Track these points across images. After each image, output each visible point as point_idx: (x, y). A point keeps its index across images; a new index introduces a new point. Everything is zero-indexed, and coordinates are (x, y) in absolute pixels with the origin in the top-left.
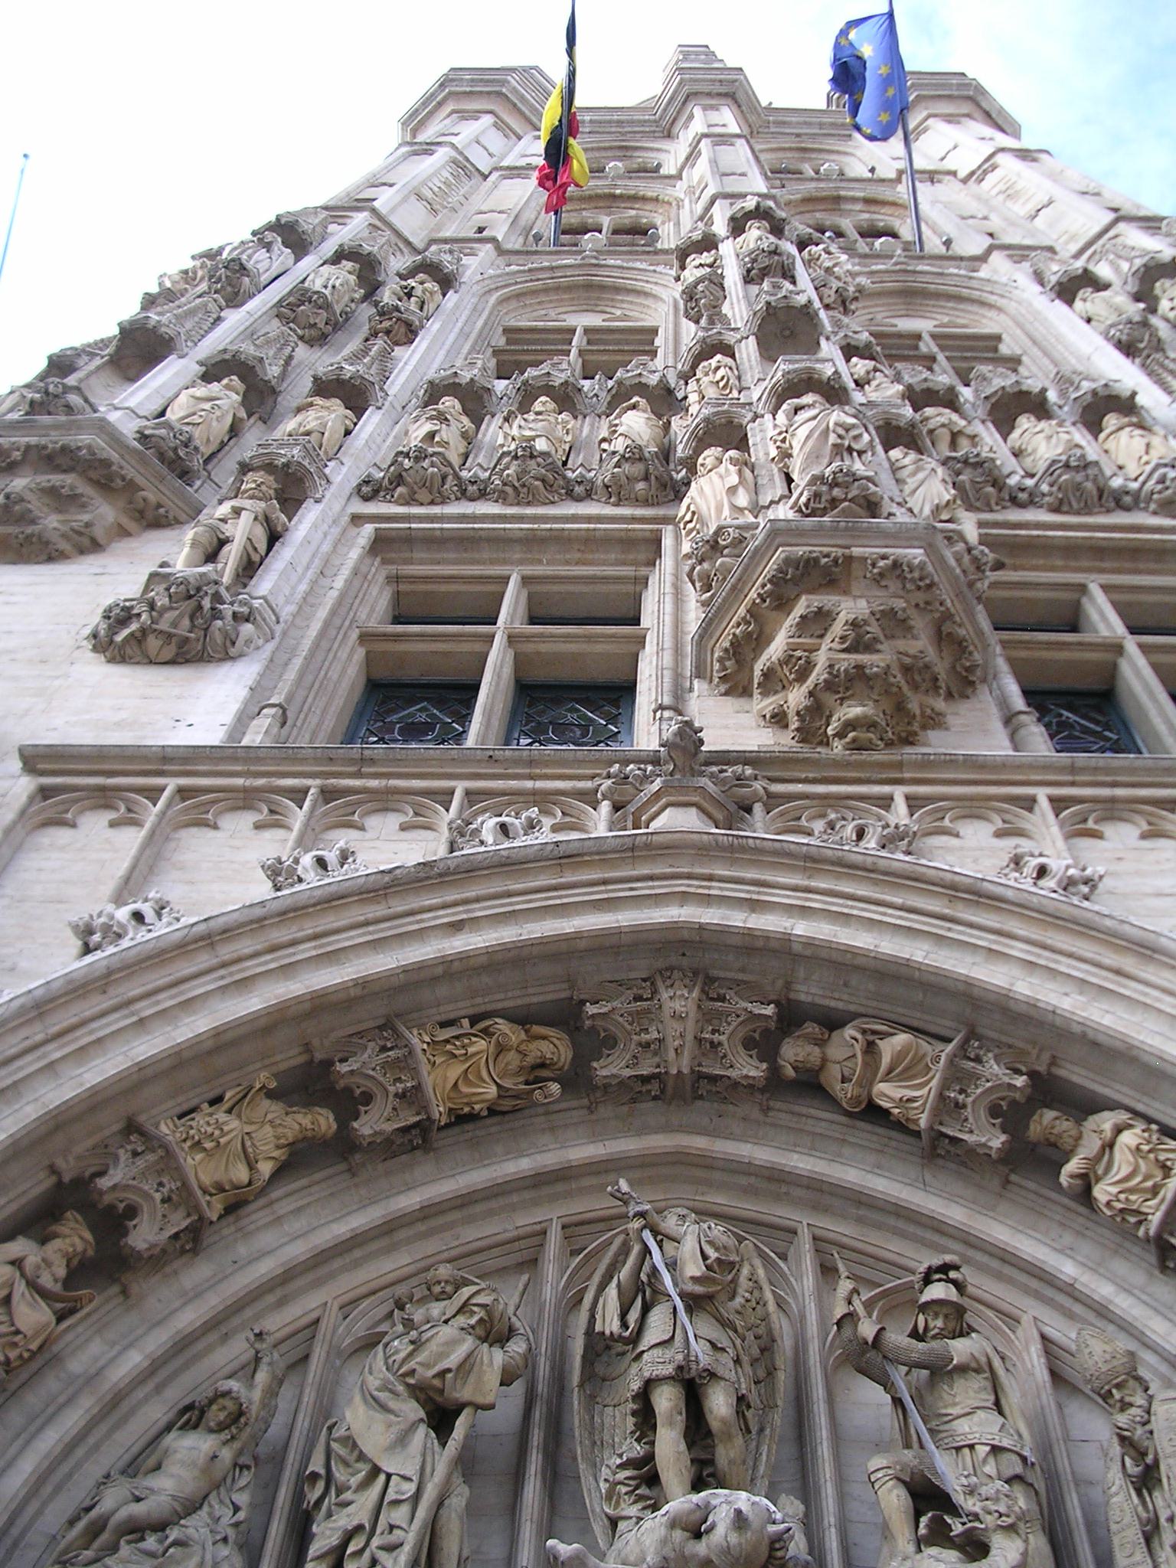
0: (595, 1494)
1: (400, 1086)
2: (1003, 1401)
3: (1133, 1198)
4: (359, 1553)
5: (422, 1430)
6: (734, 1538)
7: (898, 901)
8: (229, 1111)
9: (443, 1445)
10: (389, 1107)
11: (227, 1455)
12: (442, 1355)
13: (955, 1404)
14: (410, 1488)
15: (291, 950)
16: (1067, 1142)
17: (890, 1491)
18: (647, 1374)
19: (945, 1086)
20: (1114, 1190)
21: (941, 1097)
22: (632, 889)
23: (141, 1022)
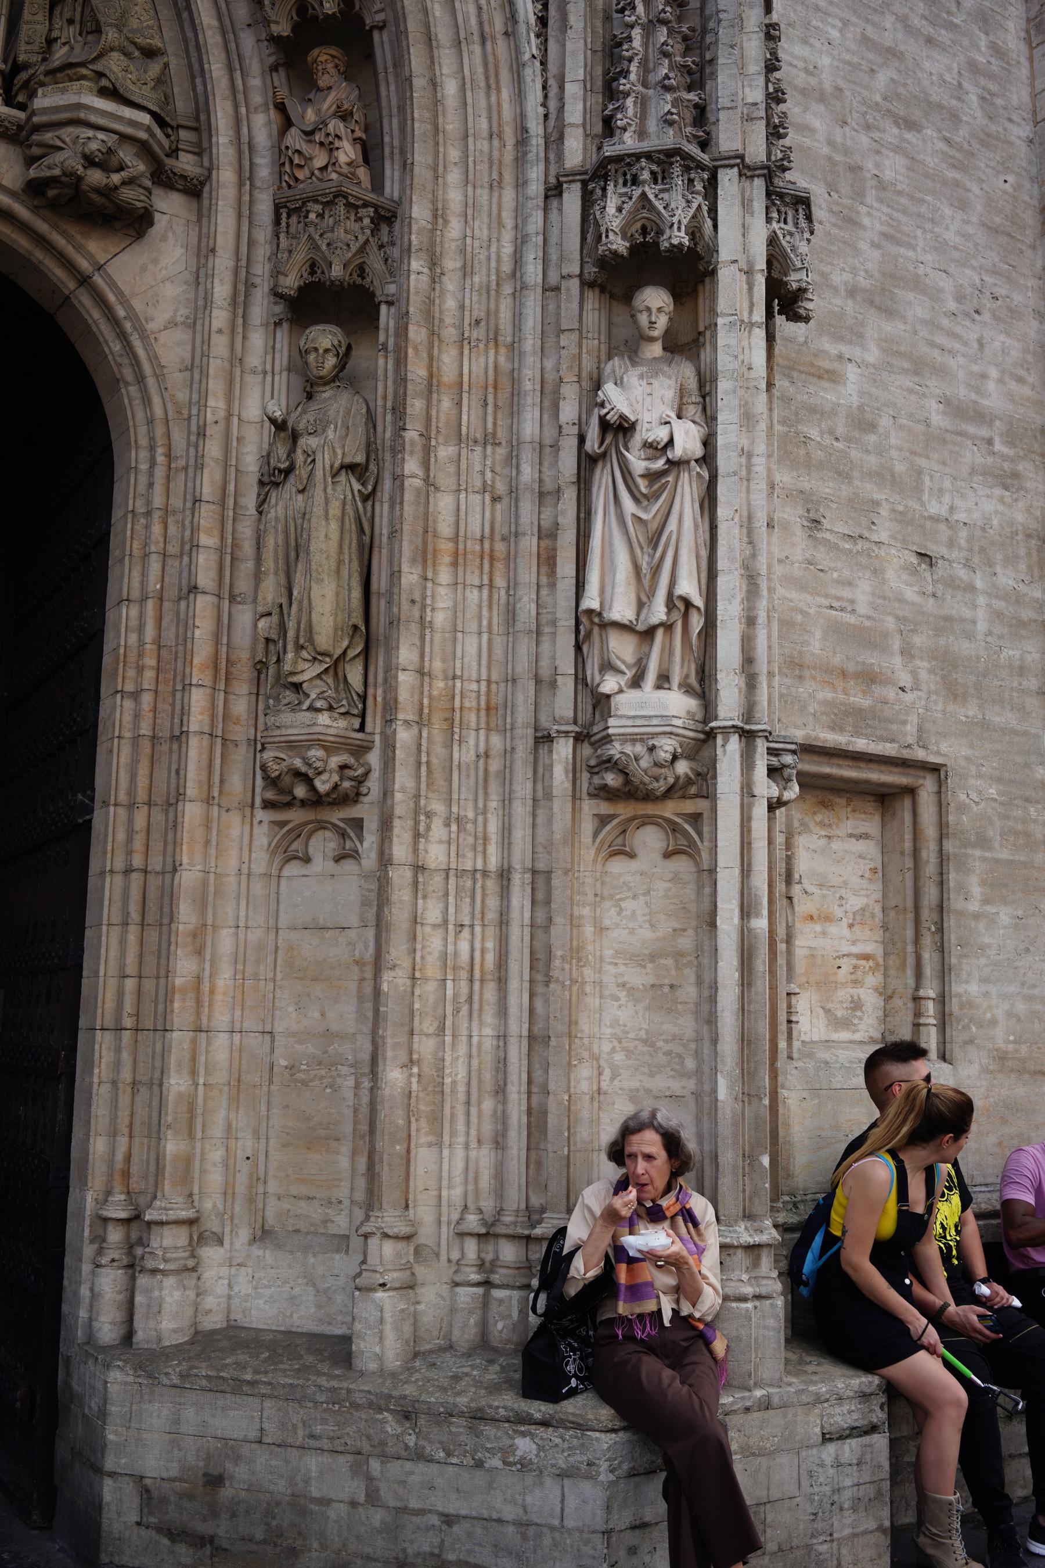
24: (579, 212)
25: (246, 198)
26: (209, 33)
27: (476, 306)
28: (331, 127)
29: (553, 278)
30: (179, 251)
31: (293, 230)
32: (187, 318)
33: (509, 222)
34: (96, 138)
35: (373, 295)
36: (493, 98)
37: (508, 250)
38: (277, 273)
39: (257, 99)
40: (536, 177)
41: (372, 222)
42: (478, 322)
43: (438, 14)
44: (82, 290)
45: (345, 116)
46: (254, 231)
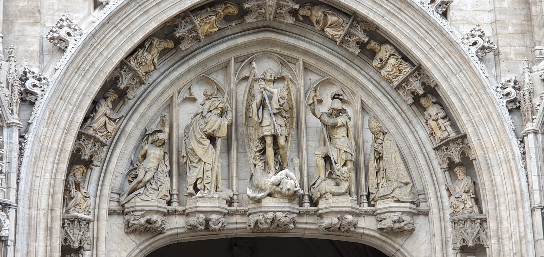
1: (192, 35)
2: (349, 133)
3: (390, 77)
5: (211, 145)
6: (287, 192)
9: (216, 150)
10: (189, 40)
11: (162, 152)
12: (213, 126)
13: (337, 135)
14: (210, 166)
16: (376, 51)
17: (320, 160)
18: (264, 134)
19: (345, 35)
20: (386, 74)
24: (541, 218)
25: (442, 215)
26: (423, 167)
27: (514, 249)
29: (537, 238)
31: (456, 228)
32: (429, 254)
33: (522, 220)
35: (484, 245)
36: (512, 181)
37: (522, 229)
38: (454, 244)
39: (441, 180)
40: (527, 205)
41: (480, 224)
42: (515, 254)
43: (491, 156)
44: (398, 252)
45: (467, 192)
46: (446, 224)
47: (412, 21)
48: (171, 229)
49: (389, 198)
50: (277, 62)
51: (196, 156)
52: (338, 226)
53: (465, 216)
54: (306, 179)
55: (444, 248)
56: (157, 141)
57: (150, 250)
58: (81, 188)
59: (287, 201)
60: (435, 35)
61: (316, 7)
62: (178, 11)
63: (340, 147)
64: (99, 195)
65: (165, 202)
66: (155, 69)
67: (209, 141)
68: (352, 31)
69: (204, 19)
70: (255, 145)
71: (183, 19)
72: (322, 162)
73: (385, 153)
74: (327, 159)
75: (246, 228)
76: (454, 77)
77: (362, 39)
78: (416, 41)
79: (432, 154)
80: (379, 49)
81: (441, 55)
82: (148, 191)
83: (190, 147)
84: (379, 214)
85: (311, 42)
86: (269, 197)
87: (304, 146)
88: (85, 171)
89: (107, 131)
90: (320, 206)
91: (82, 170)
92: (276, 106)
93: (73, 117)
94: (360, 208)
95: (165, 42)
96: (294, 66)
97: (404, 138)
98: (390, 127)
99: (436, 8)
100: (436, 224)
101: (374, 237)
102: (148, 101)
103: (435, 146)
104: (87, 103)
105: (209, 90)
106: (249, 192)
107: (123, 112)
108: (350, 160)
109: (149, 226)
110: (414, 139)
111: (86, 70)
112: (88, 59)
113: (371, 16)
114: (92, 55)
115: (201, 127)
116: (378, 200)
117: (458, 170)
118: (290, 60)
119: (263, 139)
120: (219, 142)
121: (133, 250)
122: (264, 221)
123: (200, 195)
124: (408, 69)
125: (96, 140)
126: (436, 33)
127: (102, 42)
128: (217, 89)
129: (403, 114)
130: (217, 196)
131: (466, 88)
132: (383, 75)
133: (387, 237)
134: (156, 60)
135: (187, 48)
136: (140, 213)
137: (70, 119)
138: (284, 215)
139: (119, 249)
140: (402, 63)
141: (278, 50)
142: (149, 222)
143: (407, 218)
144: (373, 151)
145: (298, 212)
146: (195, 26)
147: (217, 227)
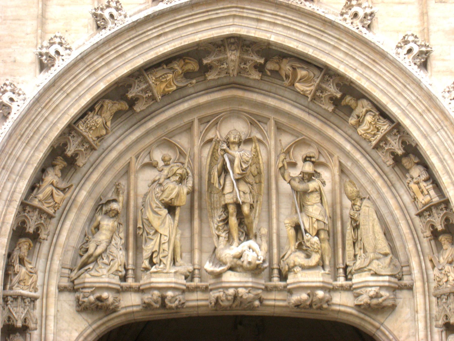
0: (213, 228)
1: (147, 95)
2: (323, 199)
4: (157, 257)
7: (307, 23)
8: (97, 114)
10: (144, 102)
11: (116, 223)
12: (171, 193)
13: (309, 201)
14: (167, 239)
15: (108, 55)
16: (353, 107)
17: (289, 230)
19: (316, 90)
20: (363, 132)
21: (315, 93)
22: (217, 14)
23: (68, 95)
25: (427, 289)
26: (407, 235)
28: (446, 268)
30: (408, 310)
31: (439, 304)
32: (413, 333)
34: (372, 290)
39: (427, 251)
47: (388, 74)
48: (126, 307)
49: (365, 271)
50: (246, 121)
51: (152, 228)
52: (308, 303)
53: (447, 290)
54: (275, 251)
55: (429, 325)
56: (110, 211)
57: (103, 328)
58: (26, 263)
59: (251, 276)
60: (414, 89)
61: (285, 61)
62: (128, 70)
63: (312, 215)
64: (48, 272)
65: (117, 278)
66: (107, 133)
67: (166, 211)
68: (324, 86)
69: (159, 77)
70: (218, 215)
71: (136, 79)
72: (292, 232)
73: (362, 220)
74: (297, 228)
75: (207, 306)
76: (435, 135)
77: (335, 94)
78: (393, 96)
79: (417, 220)
80: (355, 105)
81: (420, 111)
82: (98, 265)
83: (146, 217)
84: (355, 289)
85: (282, 99)
86: (230, 272)
87: (274, 215)
88: (32, 245)
89: (54, 201)
90: (289, 281)
91: (28, 244)
92: (238, 171)
93: (16, 188)
94: (335, 283)
95: (118, 104)
96: (265, 126)
97: (387, 204)
98: (372, 192)
99: (414, 58)
100: (419, 299)
101: (351, 314)
102: (101, 169)
103: (420, 211)
104: (30, 172)
105: (170, 154)
106: (208, 266)
107: (75, 181)
108: (323, 229)
109: (100, 304)
110: (397, 205)
111: (30, 137)
112: (33, 125)
113: (342, 69)
114: (36, 120)
115: (157, 195)
116: (354, 273)
117: (443, 238)
118: (260, 119)
119: (226, 207)
120: (178, 212)
121: (85, 330)
122: (224, 298)
123: (155, 270)
124: (385, 127)
125: (42, 212)
126: (414, 86)
127: (48, 107)
128: (180, 153)
129: (385, 177)
130: (173, 270)
131: (448, 147)
132: (360, 134)
133: (365, 314)
134: (109, 124)
135: (142, 109)
136: (89, 290)
137: (12, 190)
138: (247, 291)
139: (70, 328)
140: (379, 120)
141: (246, 108)
142: (99, 299)
143: (385, 294)
144: (350, 220)
145: (263, 287)
146: (150, 85)
147: (173, 305)
